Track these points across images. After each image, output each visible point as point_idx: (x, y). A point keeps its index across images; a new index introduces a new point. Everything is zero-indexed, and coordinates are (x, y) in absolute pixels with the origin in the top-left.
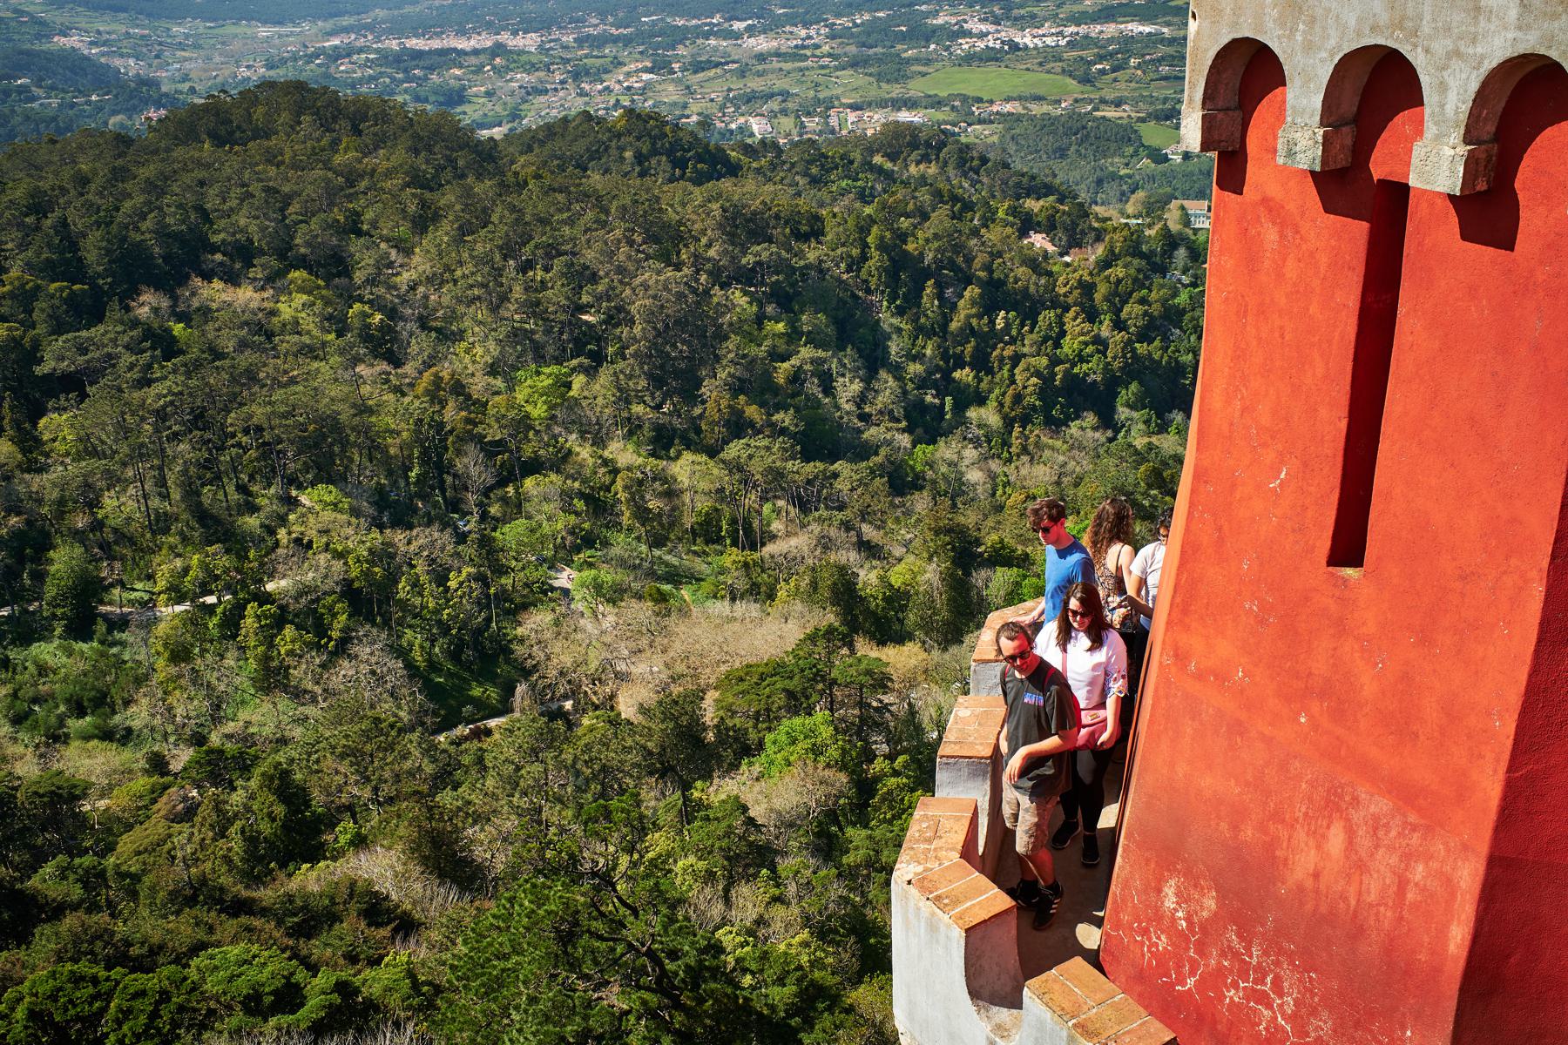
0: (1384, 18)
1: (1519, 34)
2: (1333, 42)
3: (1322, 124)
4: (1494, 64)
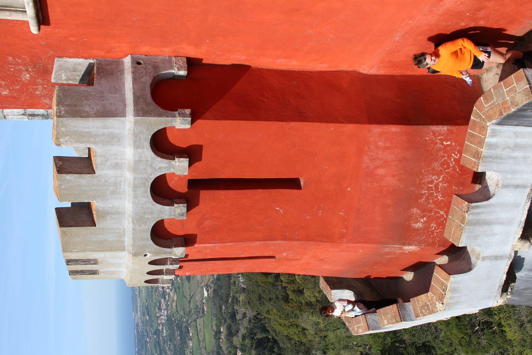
0: (143, 189)
1: (145, 148)
2: (150, 205)
3: (173, 205)
4: (153, 154)
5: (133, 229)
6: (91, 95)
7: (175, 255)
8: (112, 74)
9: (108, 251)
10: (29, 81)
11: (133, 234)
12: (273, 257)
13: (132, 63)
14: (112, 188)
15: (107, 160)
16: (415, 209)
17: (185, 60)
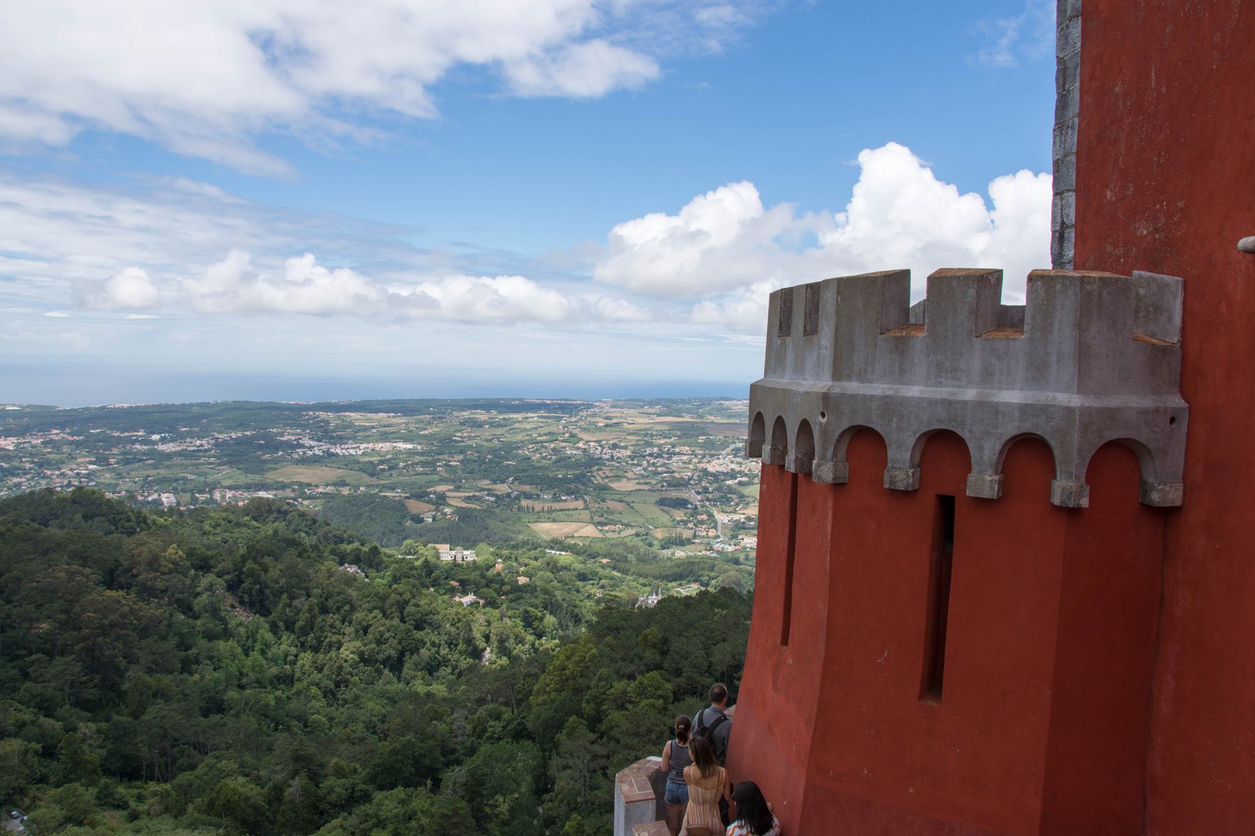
5: (872, 396)
7: (819, 466)
9: (835, 352)
12: (785, 641)
13: (1174, 410)
17: (1178, 503)
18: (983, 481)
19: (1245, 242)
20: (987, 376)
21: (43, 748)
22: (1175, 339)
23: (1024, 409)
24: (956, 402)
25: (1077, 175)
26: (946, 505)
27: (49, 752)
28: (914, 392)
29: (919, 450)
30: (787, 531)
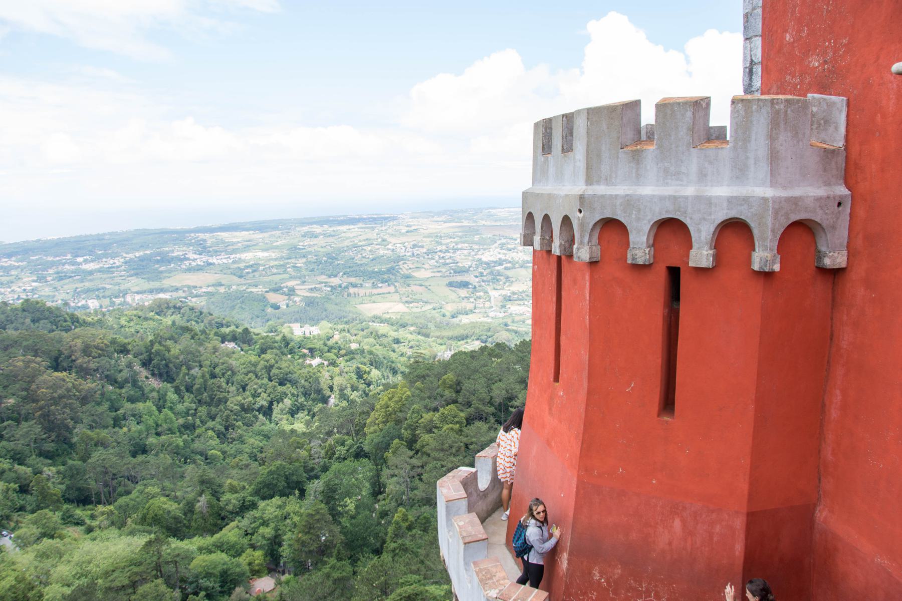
2: (649, 217)
5: (616, 196)
6: (798, 142)
7: (578, 249)
8: (825, 170)
9: (587, 164)
10: (808, 66)
11: (611, 195)
12: (557, 379)
13: (840, 196)
14: (672, 169)
15: (710, 163)
16: (619, 571)
17: (844, 265)
18: (701, 255)
19: (898, 66)
20: (702, 176)
21: (20, 487)
22: (841, 143)
23: (731, 200)
24: (679, 197)
25: (763, 24)
26: (674, 273)
27: (24, 489)
28: (645, 192)
29: (652, 234)
30: (554, 299)
